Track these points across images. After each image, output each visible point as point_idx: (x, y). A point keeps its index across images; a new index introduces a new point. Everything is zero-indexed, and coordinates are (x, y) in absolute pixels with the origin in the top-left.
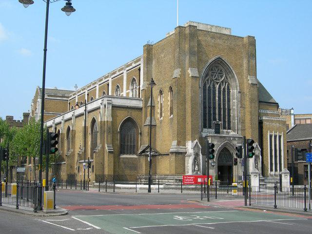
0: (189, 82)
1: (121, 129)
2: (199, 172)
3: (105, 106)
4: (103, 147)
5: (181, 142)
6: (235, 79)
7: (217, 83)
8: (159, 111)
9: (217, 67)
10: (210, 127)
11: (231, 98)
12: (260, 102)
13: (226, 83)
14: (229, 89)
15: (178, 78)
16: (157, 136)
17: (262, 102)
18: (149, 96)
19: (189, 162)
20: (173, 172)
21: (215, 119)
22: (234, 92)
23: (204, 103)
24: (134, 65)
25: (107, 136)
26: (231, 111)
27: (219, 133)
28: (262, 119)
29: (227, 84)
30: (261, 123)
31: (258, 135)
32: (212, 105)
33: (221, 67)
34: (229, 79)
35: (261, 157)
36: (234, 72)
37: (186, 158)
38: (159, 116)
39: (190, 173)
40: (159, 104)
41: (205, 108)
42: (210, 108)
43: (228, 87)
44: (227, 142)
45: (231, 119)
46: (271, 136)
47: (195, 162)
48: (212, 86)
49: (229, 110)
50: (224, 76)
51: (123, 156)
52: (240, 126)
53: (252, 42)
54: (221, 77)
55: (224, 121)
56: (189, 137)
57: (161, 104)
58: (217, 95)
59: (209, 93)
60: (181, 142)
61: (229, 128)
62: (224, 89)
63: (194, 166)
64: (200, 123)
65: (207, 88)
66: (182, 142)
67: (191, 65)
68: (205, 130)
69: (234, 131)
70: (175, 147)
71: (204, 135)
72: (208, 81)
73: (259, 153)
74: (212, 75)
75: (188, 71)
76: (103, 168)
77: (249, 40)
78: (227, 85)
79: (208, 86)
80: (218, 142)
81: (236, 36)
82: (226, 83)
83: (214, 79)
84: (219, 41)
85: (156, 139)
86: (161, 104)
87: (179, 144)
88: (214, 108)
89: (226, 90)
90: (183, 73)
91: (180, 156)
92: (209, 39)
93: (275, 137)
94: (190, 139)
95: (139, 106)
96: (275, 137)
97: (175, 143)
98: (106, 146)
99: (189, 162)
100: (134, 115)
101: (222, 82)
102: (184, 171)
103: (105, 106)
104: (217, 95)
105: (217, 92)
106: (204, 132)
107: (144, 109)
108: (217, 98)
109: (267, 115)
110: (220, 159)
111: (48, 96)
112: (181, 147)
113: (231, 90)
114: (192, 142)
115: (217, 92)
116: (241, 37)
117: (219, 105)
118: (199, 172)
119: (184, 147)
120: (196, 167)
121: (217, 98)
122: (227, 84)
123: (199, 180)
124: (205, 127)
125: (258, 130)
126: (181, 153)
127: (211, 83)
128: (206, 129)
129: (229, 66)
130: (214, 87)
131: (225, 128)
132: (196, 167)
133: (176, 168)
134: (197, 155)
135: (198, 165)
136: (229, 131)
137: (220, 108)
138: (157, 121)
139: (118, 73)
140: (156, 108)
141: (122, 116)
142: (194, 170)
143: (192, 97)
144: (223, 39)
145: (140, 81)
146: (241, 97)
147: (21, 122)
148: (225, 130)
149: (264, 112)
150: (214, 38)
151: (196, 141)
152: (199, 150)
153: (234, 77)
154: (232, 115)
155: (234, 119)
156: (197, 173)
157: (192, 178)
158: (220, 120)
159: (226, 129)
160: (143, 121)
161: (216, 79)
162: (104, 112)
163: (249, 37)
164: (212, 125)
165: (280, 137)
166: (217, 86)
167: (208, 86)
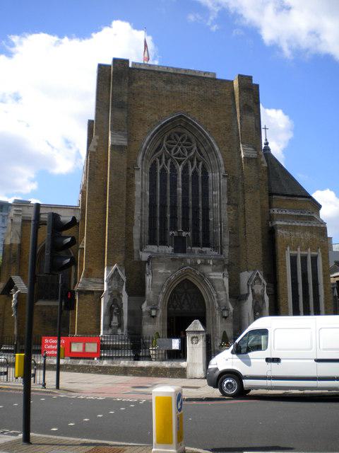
6: (216, 154)
9: (180, 134)
10: (163, 243)
13: (198, 162)
21: (174, 227)
22: (217, 178)
26: (211, 213)
27: (184, 251)
28: (274, 224)
29: (201, 164)
33: (187, 134)
41: (152, 206)
42: (163, 206)
45: (211, 229)
46: (293, 259)
48: (168, 169)
49: (206, 209)
52: (226, 240)
54: (189, 151)
55: (195, 231)
58: (180, 183)
59: (163, 181)
61: (207, 245)
62: (195, 173)
64: (147, 237)
65: (159, 171)
67: (116, 129)
69: (215, 248)
72: (160, 158)
74: (170, 149)
78: (200, 166)
82: (198, 162)
84: (180, 88)
88: (174, 207)
91: (89, 296)
92: (161, 84)
93: (304, 259)
96: (304, 259)
104: (180, 183)
105: (180, 178)
108: (180, 190)
109: (283, 217)
113: (210, 175)
115: (180, 178)
116: (228, 81)
117: (185, 200)
120: (115, 319)
121: (180, 190)
122: (201, 164)
126: (92, 292)
127: (166, 163)
130: (173, 169)
131: (196, 244)
132: (115, 319)
136: (204, 249)
137: (185, 207)
144: (190, 84)
146: (228, 184)
148: (196, 249)
150: (171, 82)
154: (211, 219)
161: (179, 155)
164: (168, 239)
165: (314, 259)
166: (180, 169)
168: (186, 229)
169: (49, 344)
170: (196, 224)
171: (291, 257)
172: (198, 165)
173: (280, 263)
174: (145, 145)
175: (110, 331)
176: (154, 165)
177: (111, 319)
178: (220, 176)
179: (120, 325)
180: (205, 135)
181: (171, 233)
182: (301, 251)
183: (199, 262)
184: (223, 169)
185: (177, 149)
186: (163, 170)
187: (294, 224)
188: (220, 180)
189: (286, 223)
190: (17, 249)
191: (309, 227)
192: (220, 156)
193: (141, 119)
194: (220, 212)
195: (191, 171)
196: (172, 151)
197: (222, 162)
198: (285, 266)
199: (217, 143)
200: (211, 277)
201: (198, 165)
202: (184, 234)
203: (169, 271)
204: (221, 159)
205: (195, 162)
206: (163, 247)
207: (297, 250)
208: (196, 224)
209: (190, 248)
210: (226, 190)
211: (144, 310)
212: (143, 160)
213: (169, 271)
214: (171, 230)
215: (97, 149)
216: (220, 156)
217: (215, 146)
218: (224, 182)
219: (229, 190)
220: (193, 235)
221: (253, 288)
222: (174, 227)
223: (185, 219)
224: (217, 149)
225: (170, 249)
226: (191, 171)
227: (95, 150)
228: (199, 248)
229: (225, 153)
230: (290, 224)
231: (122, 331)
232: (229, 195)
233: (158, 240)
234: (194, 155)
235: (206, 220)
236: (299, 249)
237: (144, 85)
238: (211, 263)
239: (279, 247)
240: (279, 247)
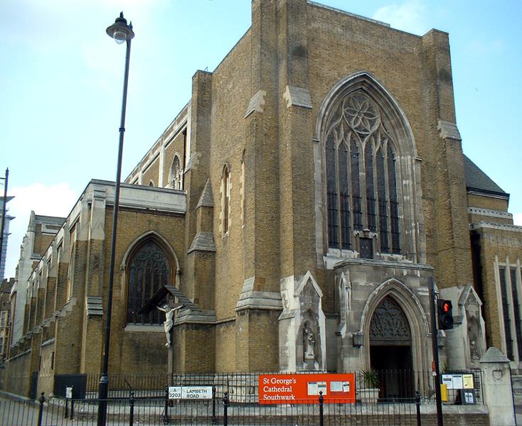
0: (287, 123)
1: (129, 261)
2: (317, 366)
3: (90, 205)
4: (80, 306)
5: (269, 279)
6: (407, 130)
7: (363, 137)
8: (222, 216)
10: (346, 246)
11: (398, 175)
12: (468, 189)
13: (383, 139)
14: (391, 155)
15: (259, 113)
16: (217, 276)
17: (474, 189)
18: (198, 185)
19: (290, 333)
20: (244, 365)
21: (358, 226)
22: (406, 161)
23: (331, 184)
24: (176, 128)
25: (90, 278)
26: (400, 208)
28: (476, 227)
29: (386, 142)
30: (476, 237)
31: (471, 265)
32: (350, 188)
33: (368, 101)
34: (390, 130)
35: (482, 322)
36: (402, 113)
37: (282, 325)
38: (221, 228)
39: (292, 368)
40: (223, 199)
41: (331, 195)
43: (389, 149)
44: (393, 283)
46: (502, 271)
47: (305, 334)
49: (394, 204)
50: (379, 121)
51: (131, 328)
52: (423, 245)
53: (439, 43)
54: (372, 123)
55: (383, 232)
56: (288, 266)
57: (226, 199)
58: (362, 165)
60: (269, 279)
61: (397, 250)
63: (301, 347)
66: (269, 282)
67: (291, 81)
68: (332, 251)
69: (409, 255)
70: (250, 294)
71: (331, 264)
72: (338, 129)
73: (477, 313)
74: (350, 118)
75: (285, 95)
76: (79, 360)
77: (435, 40)
79: (338, 143)
80: (369, 280)
81: (402, 32)
83: (353, 127)
85: (214, 285)
86: (226, 199)
87: (259, 286)
88: (357, 198)
89: (386, 156)
90: (274, 101)
91: (263, 318)
94: (292, 270)
95: (178, 208)
97: (249, 283)
98: (86, 298)
99: (290, 333)
100: (164, 229)
101: (374, 135)
102: (276, 361)
103: (90, 205)
104: (362, 165)
106: (332, 257)
107: (188, 215)
108: (362, 174)
110: (374, 325)
111: (48, 227)
112: (266, 294)
113: (397, 158)
114: (297, 279)
115: (362, 159)
118: (317, 366)
119: (275, 295)
120: (310, 350)
121: (362, 174)
123: (314, 390)
124: (333, 244)
125: (471, 261)
126: (267, 311)
128: (335, 250)
129: (389, 99)
131: (384, 249)
132: (310, 350)
133: (252, 354)
134: (310, 313)
135: (316, 344)
136: (395, 256)
138: (217, 241)
139: (152, 157)
140: (216, 209)
141: (131, 232)
142: (301, 360)
143: (294, 159)
145: (185, 157)
146: (422, 171)
147: (8, 281)
149: (478, 213)
151: (308, 275)
152: (315, 301)
153: (401, 124)
154: (401, 217)
155: (407, 227)
156: (311, 368)
157: (288, 382)
158: (372, 228)
159: (387, 252)
160: (187, 243)
162: (86, 218)
163: (435, 32)
164: (353, 241)
167: (338, 143)
168: (374, 231)
169: (271, 385)
170: (383, 223)
171: (511, 270)
172: (382, 143)
173: (488, 278)
174: (324, 109)
175: (305, 365)
176: (331, 139)
177: (305, 350)
178: (412, 160)
179: (317, 358)
180: (393, 104)
181: (356, 232)
182: (510, 263)
183: (405, 273)
184: (415, 151)
185: (357, 118)
186: (342, 144)
187: (500, 228)
188: (412, 165)
189: (492, 227)
190: (101, 248)
191: (515, 232)
192: (412, 134)
193: (318, 75)
194: (414, 207)
195: (375, 149)
196: (352, 122)
197: (414, 143)
198: (494, 280)
199: (407, 116)
200: (420, 293)
201: (382, 143)
202: (371, 235)
203: (371, 284)
204: (413, 138)
205: (379, 140)
206: (347, 251)
207: (505, 262)
208: (383, 223)
209: (378, 254)
210: (420, 179)
211: (343, 337)
212: (321, 130)
213: (371, 284)
214: (355, 229)
215: (264, 110)
216: (412, 134)
217: (406, 119)
218: (417, 168)
219: (423, 180)
220: (381, 235)
221: (468, 309)
222: (358, 226)
223: (371, 215)
224: (408, 124)
225: (356, 254)
226: (375, 149)
227: (262, 110)
228: (389, 255)
229: (416, 130)
230: (496, 227)
231: (320, 366)
232: (423, 187)
233: (340, 242)
234: (378, 130)
235: (395, 218)
236: (507, 260)
237: (319, 28)
238: (419, 275)
239: (487, 254)
240: (486, 257)
